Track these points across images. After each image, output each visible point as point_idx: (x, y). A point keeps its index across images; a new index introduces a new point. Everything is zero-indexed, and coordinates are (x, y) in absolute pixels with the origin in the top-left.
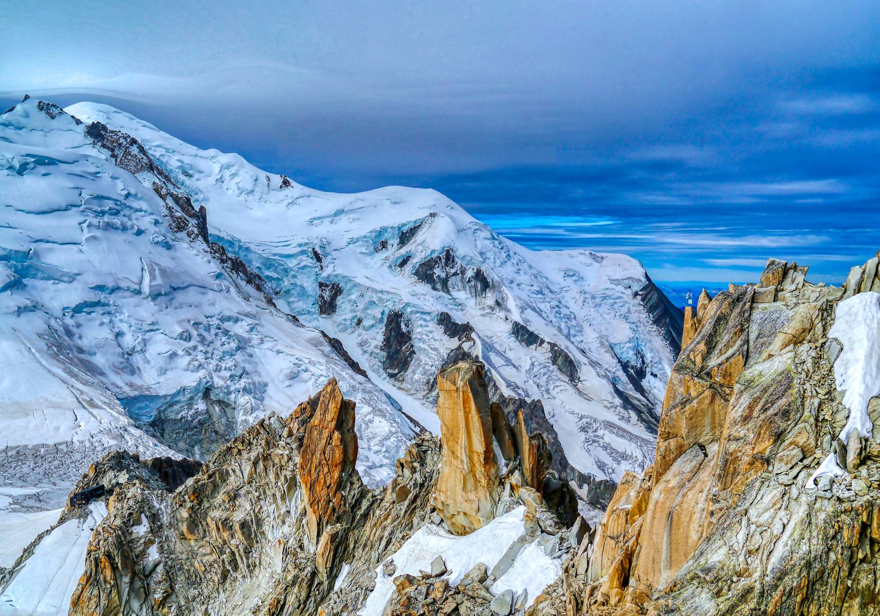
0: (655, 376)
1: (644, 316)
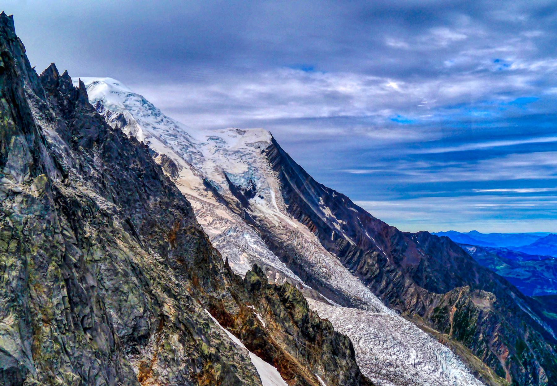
0: (262, 198)
1: (266, 164)
